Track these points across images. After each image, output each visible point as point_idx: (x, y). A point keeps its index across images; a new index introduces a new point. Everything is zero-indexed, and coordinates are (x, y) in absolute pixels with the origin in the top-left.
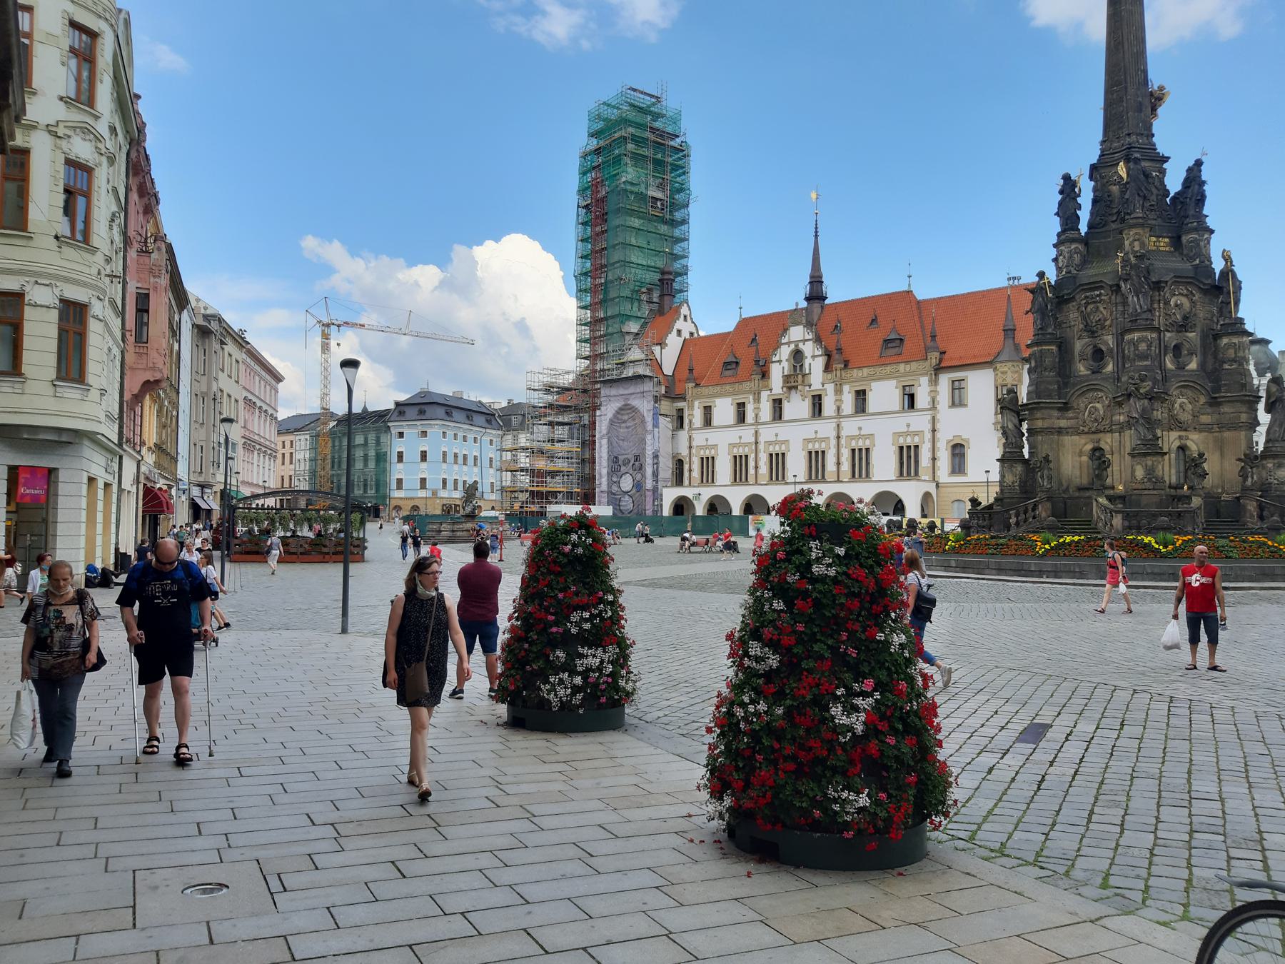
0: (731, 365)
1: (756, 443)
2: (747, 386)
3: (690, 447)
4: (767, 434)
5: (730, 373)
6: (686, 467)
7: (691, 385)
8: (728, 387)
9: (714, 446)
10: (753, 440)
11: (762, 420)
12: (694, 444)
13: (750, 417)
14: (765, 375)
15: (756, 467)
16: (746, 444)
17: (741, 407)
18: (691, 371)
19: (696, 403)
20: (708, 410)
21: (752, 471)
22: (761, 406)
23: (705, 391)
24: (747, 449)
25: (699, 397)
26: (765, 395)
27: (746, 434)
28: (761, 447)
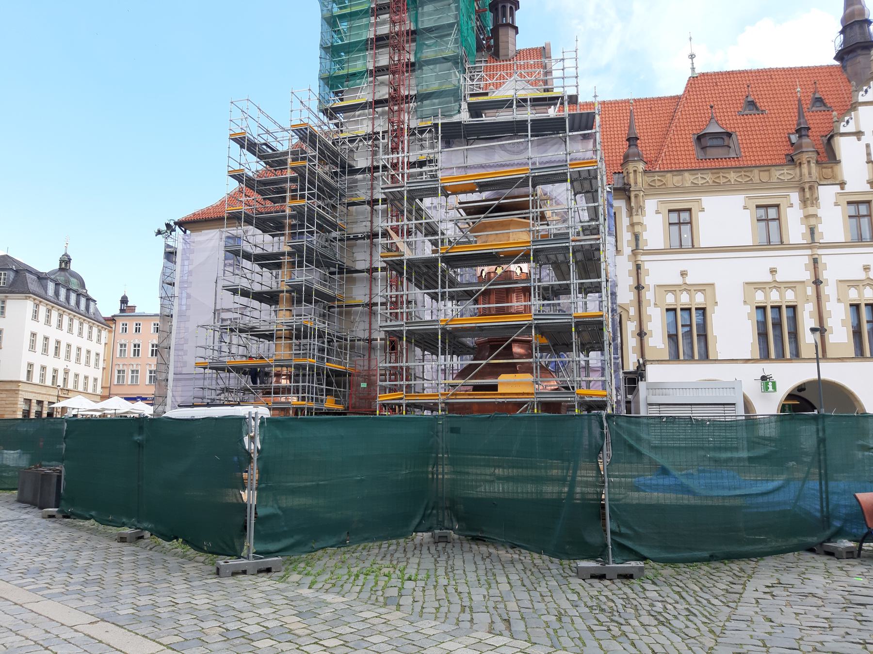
0: (712, 144)
1: (817, 282)
2: (786, 173)
3: (639, 288)
4: (841, 266)
5: (712, 153)
6: (631, 327)
7: (641, 166)
8: (732, 176)
9: (706, 288)
10: (807, 276)
11: (827, 238)
12: (649, 281)
13: (796, 232)
14: (828, 156)
15: (820, 330)
16: (792, 285)
17: (768, 215)
18: (632, 140)
19: (651, 205)
20: (682, 219)
21: (808, 339)
22: (820, 212)
23: (672, 180)
24: (790, 297)
25: (653, 190)
26: (827, 193)
27: (794, 267)
28: (829, 290)
